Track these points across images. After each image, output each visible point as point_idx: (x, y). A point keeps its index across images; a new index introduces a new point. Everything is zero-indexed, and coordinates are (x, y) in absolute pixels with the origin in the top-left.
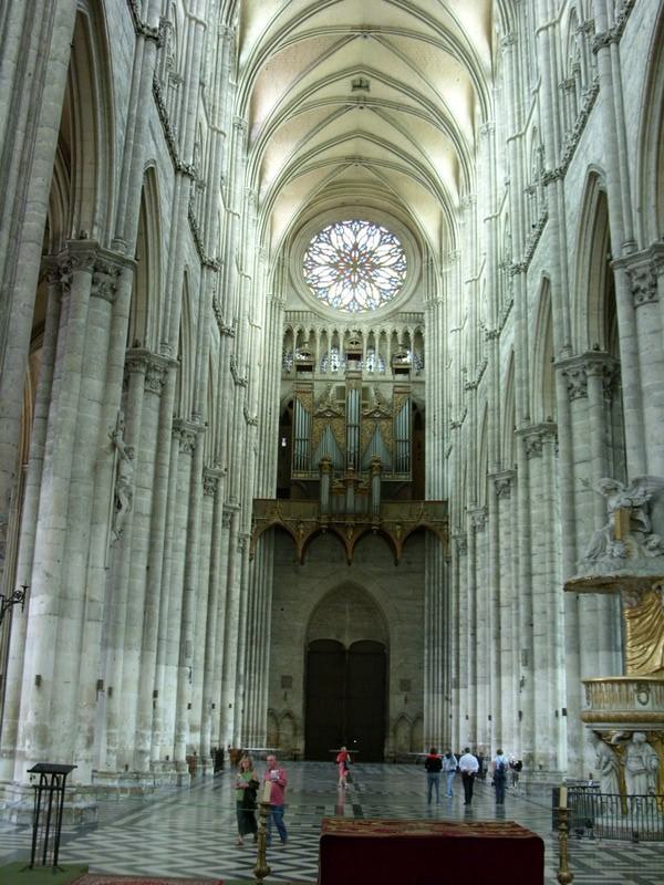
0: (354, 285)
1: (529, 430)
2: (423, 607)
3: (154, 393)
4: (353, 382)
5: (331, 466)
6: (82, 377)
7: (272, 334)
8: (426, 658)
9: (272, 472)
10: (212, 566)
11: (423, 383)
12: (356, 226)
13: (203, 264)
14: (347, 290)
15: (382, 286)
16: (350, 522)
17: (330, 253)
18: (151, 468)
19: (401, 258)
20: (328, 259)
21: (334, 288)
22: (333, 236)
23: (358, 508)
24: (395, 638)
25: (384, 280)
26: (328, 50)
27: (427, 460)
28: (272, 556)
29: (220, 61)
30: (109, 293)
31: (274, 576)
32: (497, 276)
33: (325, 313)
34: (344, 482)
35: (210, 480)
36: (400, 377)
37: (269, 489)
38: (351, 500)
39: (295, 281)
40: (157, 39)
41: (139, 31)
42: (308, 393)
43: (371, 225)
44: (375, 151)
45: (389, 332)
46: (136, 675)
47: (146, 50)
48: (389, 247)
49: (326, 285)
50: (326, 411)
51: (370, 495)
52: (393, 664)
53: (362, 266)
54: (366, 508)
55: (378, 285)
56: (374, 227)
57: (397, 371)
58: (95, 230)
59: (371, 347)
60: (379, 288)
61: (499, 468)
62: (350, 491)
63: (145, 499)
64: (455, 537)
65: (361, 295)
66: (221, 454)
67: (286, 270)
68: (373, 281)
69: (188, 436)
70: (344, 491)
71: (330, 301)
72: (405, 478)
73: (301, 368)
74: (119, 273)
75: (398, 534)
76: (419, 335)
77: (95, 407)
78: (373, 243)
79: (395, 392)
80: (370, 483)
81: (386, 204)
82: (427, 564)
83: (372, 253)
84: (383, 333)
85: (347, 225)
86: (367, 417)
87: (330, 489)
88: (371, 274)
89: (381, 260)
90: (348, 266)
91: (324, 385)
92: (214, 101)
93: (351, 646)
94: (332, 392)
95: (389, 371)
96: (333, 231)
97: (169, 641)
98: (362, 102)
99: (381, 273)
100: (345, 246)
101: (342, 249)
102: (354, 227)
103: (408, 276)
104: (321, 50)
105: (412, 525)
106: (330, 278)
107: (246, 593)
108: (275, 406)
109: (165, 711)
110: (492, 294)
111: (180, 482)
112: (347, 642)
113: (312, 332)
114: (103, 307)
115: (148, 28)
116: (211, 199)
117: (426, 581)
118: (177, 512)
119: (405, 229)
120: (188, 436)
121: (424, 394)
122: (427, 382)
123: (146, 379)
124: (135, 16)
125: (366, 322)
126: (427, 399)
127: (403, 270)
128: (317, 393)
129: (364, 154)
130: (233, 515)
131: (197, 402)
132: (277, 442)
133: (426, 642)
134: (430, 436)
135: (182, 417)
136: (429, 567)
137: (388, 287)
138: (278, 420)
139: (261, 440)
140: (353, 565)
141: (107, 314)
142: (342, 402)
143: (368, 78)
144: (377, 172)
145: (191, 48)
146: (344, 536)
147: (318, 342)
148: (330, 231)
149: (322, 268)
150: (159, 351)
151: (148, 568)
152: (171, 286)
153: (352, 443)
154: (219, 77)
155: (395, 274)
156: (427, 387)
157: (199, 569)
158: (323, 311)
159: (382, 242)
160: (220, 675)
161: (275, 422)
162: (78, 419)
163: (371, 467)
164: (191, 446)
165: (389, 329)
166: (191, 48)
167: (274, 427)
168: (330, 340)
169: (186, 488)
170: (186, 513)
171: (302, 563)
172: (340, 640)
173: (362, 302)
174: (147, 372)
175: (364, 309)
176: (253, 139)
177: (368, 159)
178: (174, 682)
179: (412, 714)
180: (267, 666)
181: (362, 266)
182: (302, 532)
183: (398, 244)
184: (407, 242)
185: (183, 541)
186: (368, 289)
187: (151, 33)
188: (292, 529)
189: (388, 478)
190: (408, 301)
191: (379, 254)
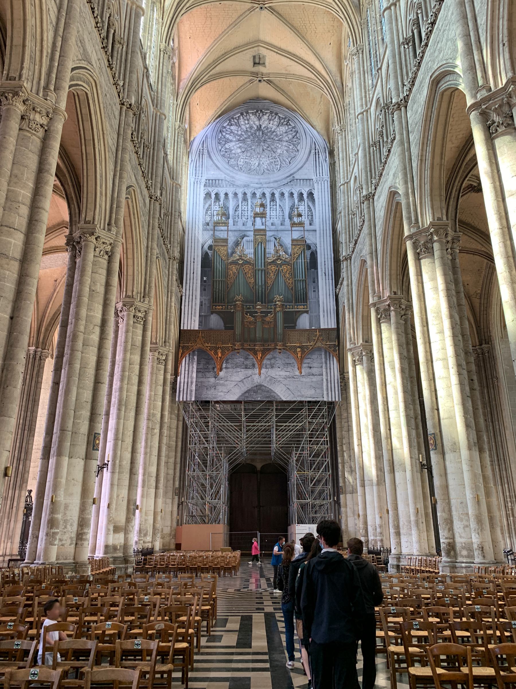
1: (420, 232)
10: (140, 382)
18: (25, 211)
32: (370, 154)
35: (139, 311)
61: (380, 297)
93: (262, 467)
97: (74, 433)
110: (366, 167)
111: (94, 282)
118: (89, 309)
120: (103, 243)
131: (114, 216)
151: (12, 318)
152: (60, 39)
157: (128, 383)
160: (154, 484)
164: (107, 253)
169: (100, 289)
170: (100, 312)
185: (95, 337)
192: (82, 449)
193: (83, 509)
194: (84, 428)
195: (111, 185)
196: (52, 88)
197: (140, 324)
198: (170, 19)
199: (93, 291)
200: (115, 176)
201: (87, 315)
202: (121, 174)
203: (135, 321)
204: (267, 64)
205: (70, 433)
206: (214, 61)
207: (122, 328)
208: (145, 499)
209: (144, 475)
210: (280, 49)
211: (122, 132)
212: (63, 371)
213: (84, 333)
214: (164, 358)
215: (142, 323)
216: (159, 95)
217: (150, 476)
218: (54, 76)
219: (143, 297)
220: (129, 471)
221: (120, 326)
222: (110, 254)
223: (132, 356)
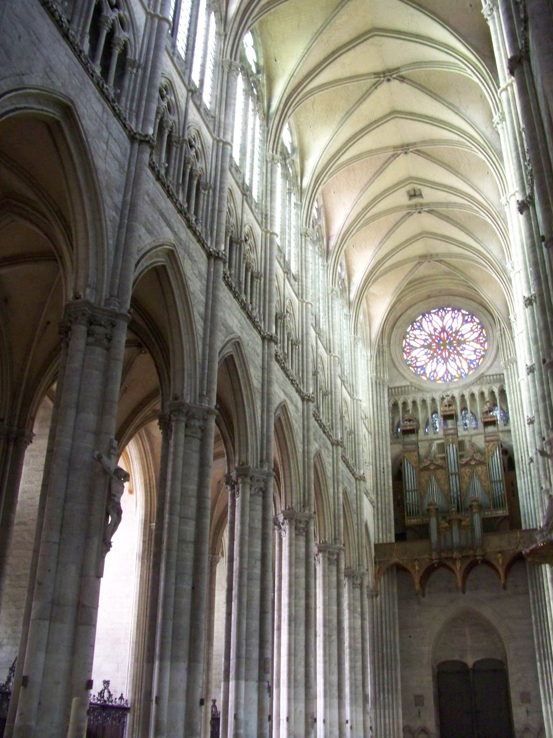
0: (446, 360)
2: (531, 624)
3: (194, 437)
4: (450, 438)
5: (437, 510)
6: (77, 412)
7: (378, 407)
8: (539, 670)
9: (390, 520)
10: (308, 596)
11: (509, 431)
12: (442, 312)
13: (263, 338)
14: (440, 365)
15: (469, 358)
16: (456, 555)
17: (424, 337)
18: (193, 502)
19: (482, 332)
20: (422, 343)
21: (429, 364)
22: (424, 323)
24: (511, 656)
25: (469, 353)
26: (379, 170)
27: (520, 496)
28: (395, 590)
29: (269, 180)
30: (105, 342)
31: (399, 608)
33: (425, 385)
34: (449, 522)
35: (300, 522)
36: (490, 429)
37: (389, 535)
38: (456, 537)
39: (397, 364)
40: (148, 142)
41: (132, 137)
42: (414, 451)
43: (453, 310)
44: (441, 247)
45: (477, 394)
46: (183, 685)
47: (140, 152)
48: (471, 324)
49: (423, 363)
50: (430, 465)
51: (473, 530)
52: (512, 679)
53: (451, 344)
55: (465, 356)
56: (456, 311)
57: (487, 424)
58: (88, 291)
59: (464, 408)
60: (466, 359)
63: (188, 528)
65: (452, 368)
66: (309, 499)
67: (387, 355)
68: (461, 355)
69: (258, 481)
70: (450, 529)
71: (428, 375)
72: (501, 513)
73: (406, 432)
74: (113, 326)
75: (500, 562)
76: (502, 392)
77: (90, 437)
78: (457, 324)
79: (486, 441)
80: (472, 520)
81: (462, 289)
83: (457, 332)
84: (472, 395)
85: (435, 313)
86: (467, 464)
87: (438, 529)
88: (458, 349)
89: (466, 337)
90: (438, 346)
91: (427, 444)
92: (266, 211)
93: (474, 665)
94: (433, 448)
95: (481, 425)
96: (424, 320)
98: (419, 208)
100: (435, 330)
101: (433, 333)
102: (440, 313)
103: (488, 345)
104: (374, 170)
105: (512, 552)
106: (425, 357)
107: (367, 624)
108: (388, 466)
109: (247, 723)
112: (470, 661)
113: (414, 403)
114: (99, 352)
115: (140, 135)
116: (268, 286)
117: (531, 601)
119: (481, 308)
121: (512, 440)
122: (512, 429)
123: (186, 426)
124: (124, 126)
125: (458, 387)
126: (514, 443)
127: (485, 342)
128: (422, 451)
129: (433, 252)
130: (338, 555)
132: (391, 495)
133: (537, 656)
134: (520, 474)
135: (249, 464)
136: (532, 587)
137: (473, 357)
138: (391, 477)
140: (468, 593)
141: (101, 359)
142: (443, 455)
143: (419, 187)
144: (449, 265)
145: (220, 163)
146: (453, 567)
147: (420, 409)
148: (421, 319)
149: (418, 350)
150: (197, 403)
151: (193, 588)
152: (207, 348)
153: (454, 489)
154: (269, 192)
155: (478, 346)
156: (512, 433)
157: (295, 598)
158: (421, 384)
159: (465, 322)
160: (336, 694)
161: (388, 479)
162: (72, 448)
163: (471, 506)
164: (261, 489)
165: (476, 390)
166: (220, 163)
167: (388, 483)
168: (429, 406)
170: (260, 547)
171: (424, 595)
172: (464, 660)
173: (454, 373)
174: (188, 420)
175: (455, 377)
176: (331, 248)
177: (437, 255)
178: (254, 696)
179: (535, 725)
180: (399, 687)
181: (451, 344)
182: (417, 568)
183: (478, 321)
184: (484, 318)
185: (257, 571)
186: (458, 361)
187: (142, 138)
188: (409, 567)
189: (488, 514)
190: (491, 365)
191: (463, 333)
192: (255, 672)
193: (260, 725)
194: (255, 654)
195: (260, 422)
196: (205, 393)
197: (302, 535)
198: (308, 200)
199: (252, 528)
200: (262, 411)
201: (249, 551)
202: (268, 408)
203: (297, 533)
204: (423, 194)
205: (244, 660)
206: (363, 209)
207: (285, 541)
208: (328, 710)
209: (325, 684)
210: (434, 183)
211: (266, 366)
212: (233, 603)
213: (248, 569)
214: (335, 557)
215: (304, 534)
216: (304, 284)
217: (331, 685)
218: (205, 382)
219: (303, 506)
220: (304, 685)
221: (284, 539)
222: (264, 489)
223: (297, 570)
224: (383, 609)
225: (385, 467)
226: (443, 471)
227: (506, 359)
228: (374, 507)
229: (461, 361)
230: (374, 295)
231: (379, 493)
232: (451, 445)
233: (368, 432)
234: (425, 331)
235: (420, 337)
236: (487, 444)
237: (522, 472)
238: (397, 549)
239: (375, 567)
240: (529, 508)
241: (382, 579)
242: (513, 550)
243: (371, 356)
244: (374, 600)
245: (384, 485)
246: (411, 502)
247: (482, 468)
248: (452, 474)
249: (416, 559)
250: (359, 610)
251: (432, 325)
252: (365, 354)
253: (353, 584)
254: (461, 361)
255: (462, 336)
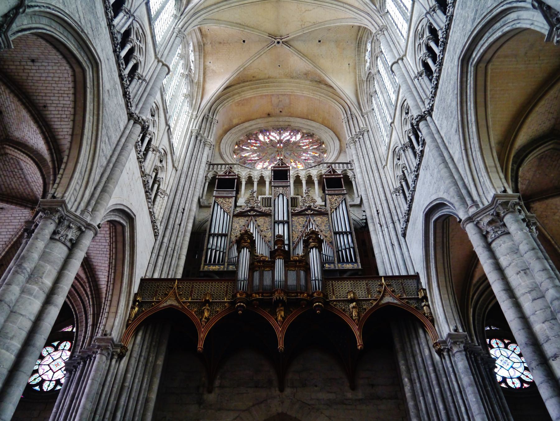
4: (281, 190)
17: (257, 145)
20: (255, 148)
22: (261, 137)
23: (292, 281)
27: (376, 251)
28: (160, 362)
39: (225, 156)
50: (249, 211)
51: (307, 269)
54: (303, 282)
62: (279, 263)
64: (470, 219)
70: (271, 265)
72: (349, 266)
82: (403, 368)
99: (304, 154)
117: (408, 394)
119: (323, 127)
129: (284, 32)
136: (409, 371)
139: (166, 228)
165: (314, 173)
182: (206, 314)
224: (127, 384)
225: (186, 208)
226: (267, 219)
227: (354, 133)
228: (156, 235)
229: (296, 164)
230: (213, 70)
231: (170, 227)
232: (281, 196)
233: (173, 166)
234: (260, 141)
235: (254, 145)
236: (330, 197)
237: (379, 225)
238: (178, 288)
239: (133, 308)
240: (393, 261)
241: (140, 334)
242: (375, 300)
243: (197, 117)
244: (114, 361)
245: (180, 225)
246: (214, 247)
247: (321, 218)
248: (279, 222)
249: (207, 301)
250: (48, 282)
251: (269, 138)
252: (191, 112)
253: (55, 233)
254: (296, 164)
255: (300, 146)
